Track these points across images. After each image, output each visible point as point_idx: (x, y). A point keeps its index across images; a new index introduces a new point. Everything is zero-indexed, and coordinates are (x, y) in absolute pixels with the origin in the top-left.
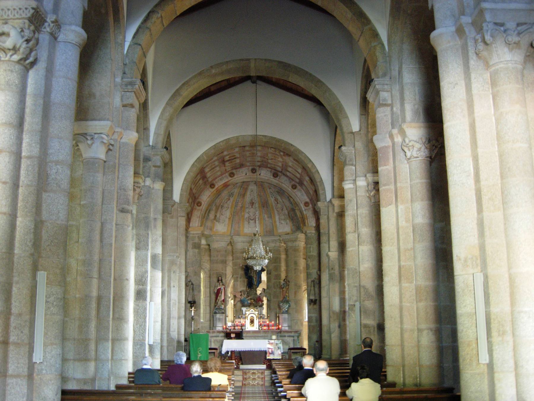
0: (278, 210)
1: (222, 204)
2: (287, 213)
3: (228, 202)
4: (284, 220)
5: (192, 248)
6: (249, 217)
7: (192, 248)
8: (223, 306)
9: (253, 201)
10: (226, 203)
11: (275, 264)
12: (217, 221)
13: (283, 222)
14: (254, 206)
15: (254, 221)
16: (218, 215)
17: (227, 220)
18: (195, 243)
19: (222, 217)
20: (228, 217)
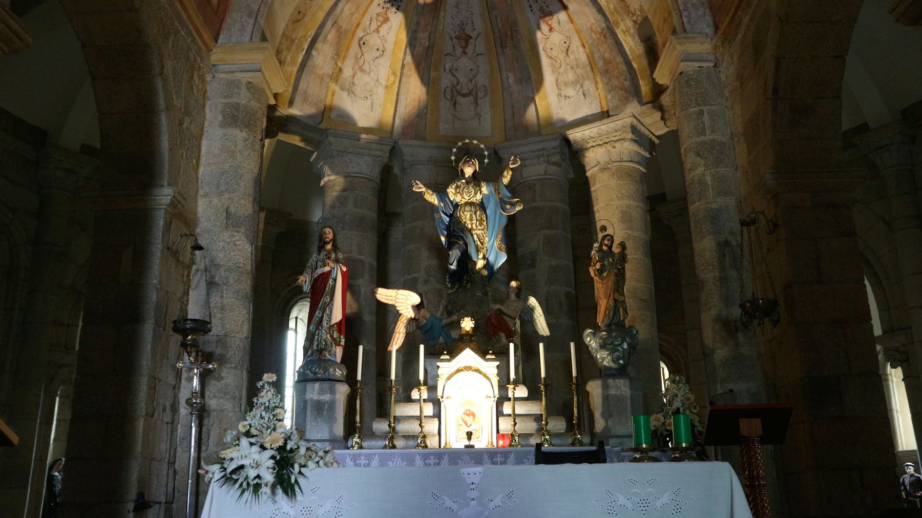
0: (554, 54)
1: (360, 33)
2: (583, 58)
3: (383, 30)
4: (575, 83)
5: (223, 125)
6: (454, 86)
7: (223, 125)
8: (339, 352)
9: (468, 30)
10: (377, 31)
11: (548, 232)
12: (342, 89)
13: (570, 92)
14: (470, 50)
15: (471, 98)
16: (347, 71)
17: (381, 91)
18: (236, 107)
19: (361, 79)
20: (384, 83)
